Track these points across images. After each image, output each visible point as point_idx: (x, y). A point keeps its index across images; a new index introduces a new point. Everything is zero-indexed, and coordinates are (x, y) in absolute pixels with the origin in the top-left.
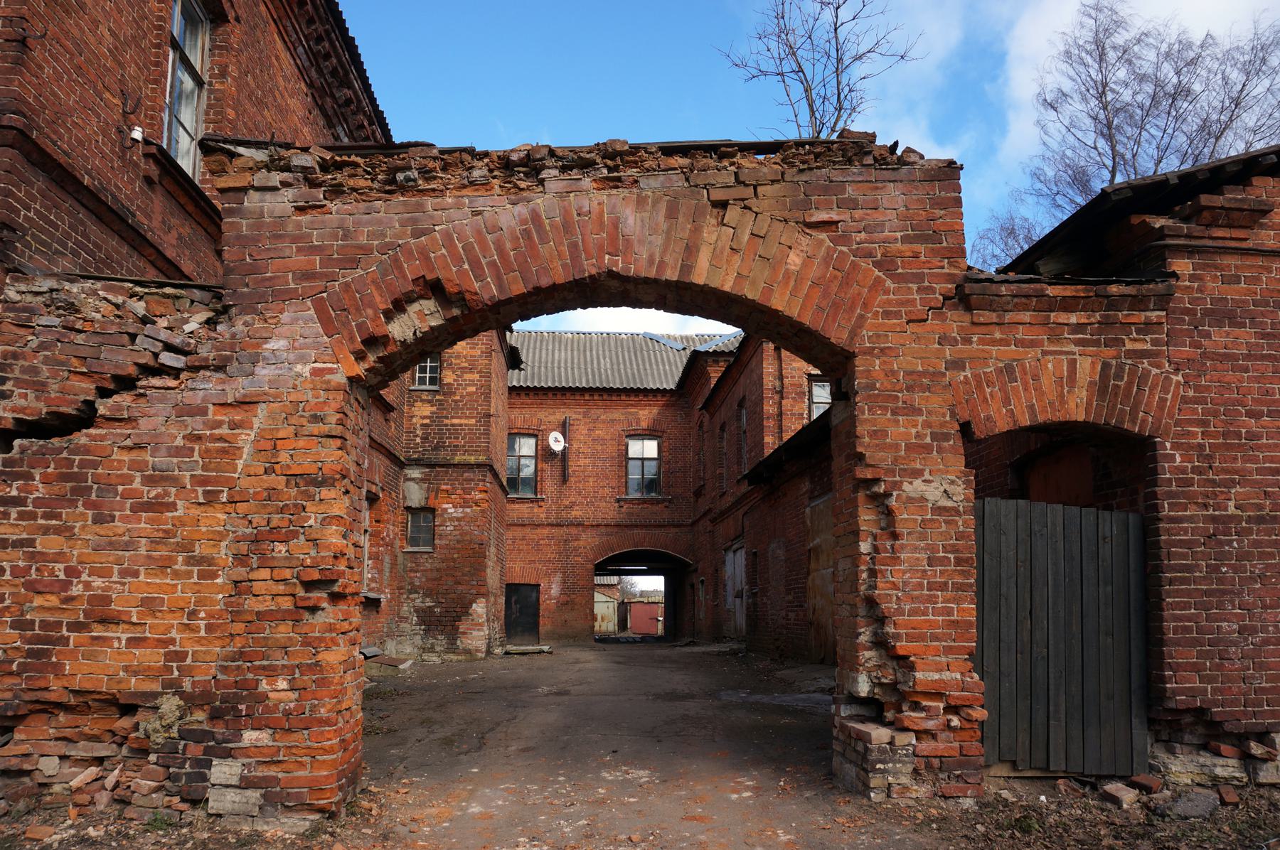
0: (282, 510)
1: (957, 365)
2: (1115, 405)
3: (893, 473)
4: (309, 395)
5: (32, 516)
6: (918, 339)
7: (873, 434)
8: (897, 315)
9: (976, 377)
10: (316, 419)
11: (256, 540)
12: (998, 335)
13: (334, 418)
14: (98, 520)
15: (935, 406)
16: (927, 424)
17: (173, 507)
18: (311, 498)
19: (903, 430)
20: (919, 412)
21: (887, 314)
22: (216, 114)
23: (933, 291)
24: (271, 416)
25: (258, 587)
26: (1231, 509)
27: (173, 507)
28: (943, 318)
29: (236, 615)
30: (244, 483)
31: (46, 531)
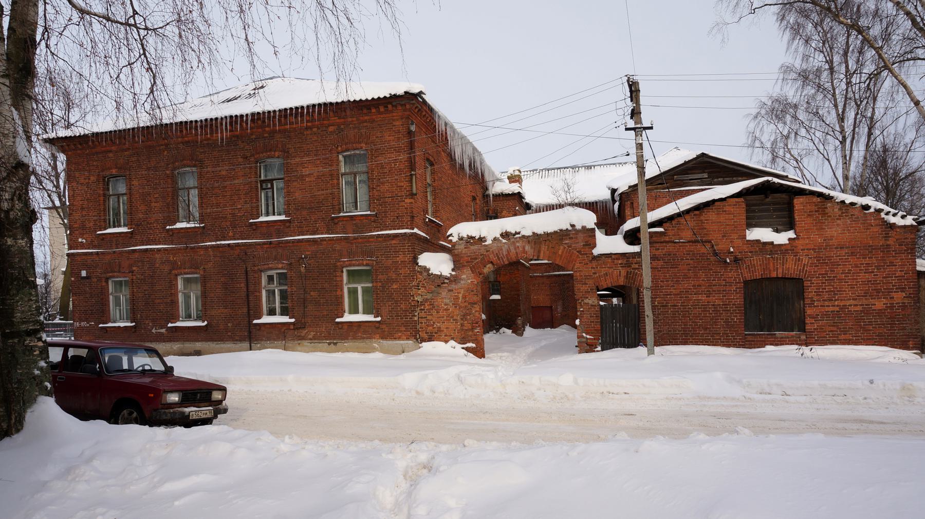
0: (468, 309)
1: (595, 273)
2: (629, 281)
3: (582, 297)
4: (471, 286)
5: (426, 312)
6: (586, 268)
7: (578, 289)
8: (582, 263)
9: (599, 276)
10: (472, 291)
11: (464, 315)
12: (603, 266)
13: (475, 291)
14: (437, 312)
15: (591, 282)
16: (589, 287)
17: (449, 310)
18: (473, 307)
19: (584, 288)
20: (587, 284)
21: (580, 263)
22: (435, 192)
23: (589, 257)
24: (464, 291)
25: (465, 325)
26: (656, 303)
27: (449, 310)
28: (591, 263)
29: (462, 330)
30: (461, 304)
31: (429, 315)
